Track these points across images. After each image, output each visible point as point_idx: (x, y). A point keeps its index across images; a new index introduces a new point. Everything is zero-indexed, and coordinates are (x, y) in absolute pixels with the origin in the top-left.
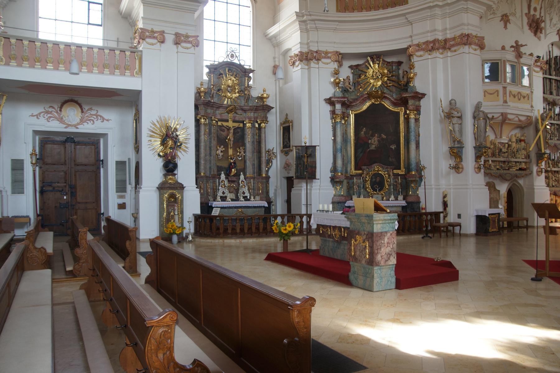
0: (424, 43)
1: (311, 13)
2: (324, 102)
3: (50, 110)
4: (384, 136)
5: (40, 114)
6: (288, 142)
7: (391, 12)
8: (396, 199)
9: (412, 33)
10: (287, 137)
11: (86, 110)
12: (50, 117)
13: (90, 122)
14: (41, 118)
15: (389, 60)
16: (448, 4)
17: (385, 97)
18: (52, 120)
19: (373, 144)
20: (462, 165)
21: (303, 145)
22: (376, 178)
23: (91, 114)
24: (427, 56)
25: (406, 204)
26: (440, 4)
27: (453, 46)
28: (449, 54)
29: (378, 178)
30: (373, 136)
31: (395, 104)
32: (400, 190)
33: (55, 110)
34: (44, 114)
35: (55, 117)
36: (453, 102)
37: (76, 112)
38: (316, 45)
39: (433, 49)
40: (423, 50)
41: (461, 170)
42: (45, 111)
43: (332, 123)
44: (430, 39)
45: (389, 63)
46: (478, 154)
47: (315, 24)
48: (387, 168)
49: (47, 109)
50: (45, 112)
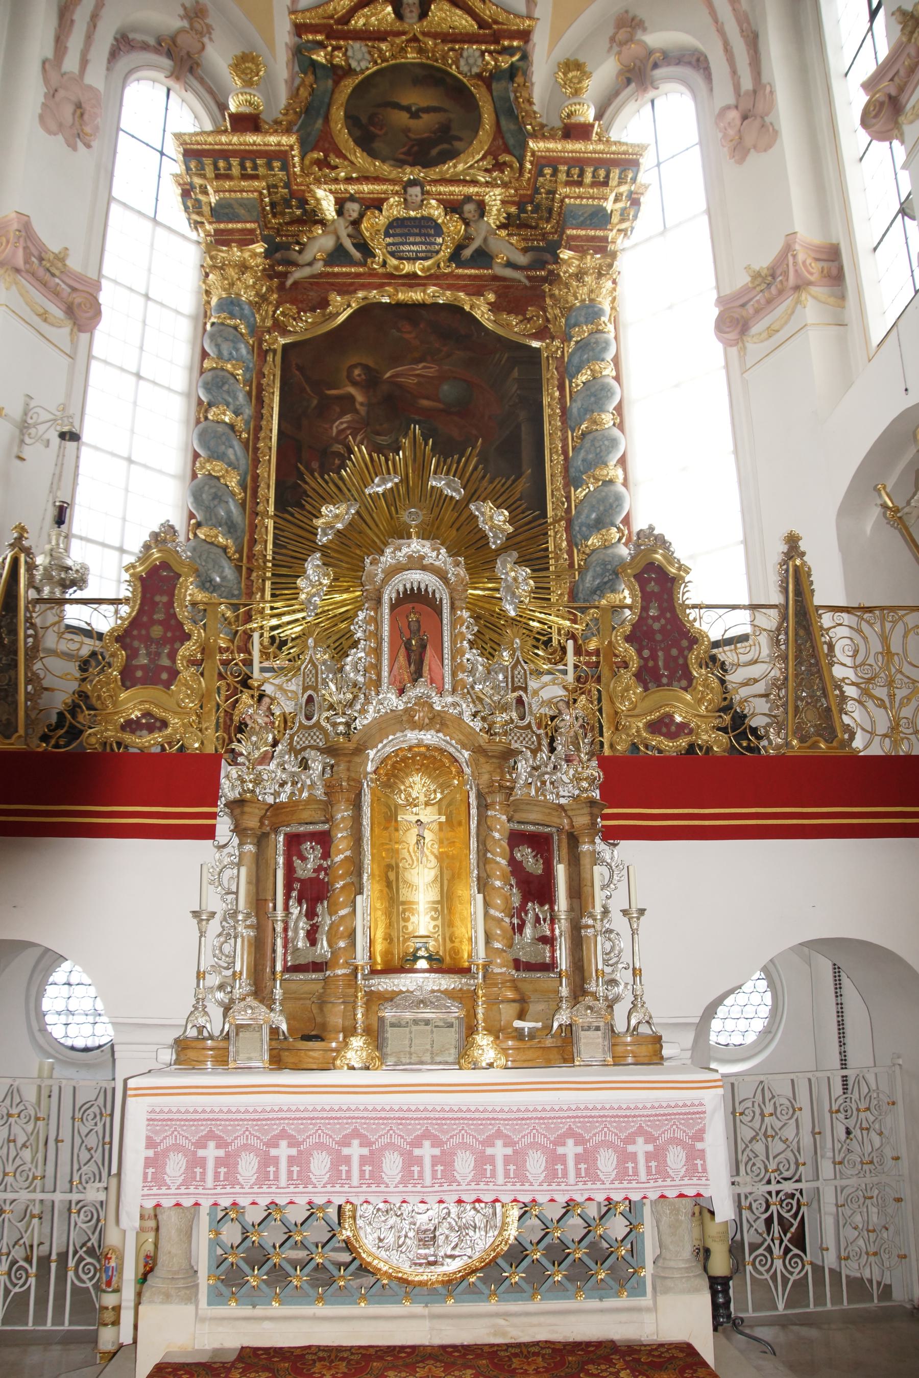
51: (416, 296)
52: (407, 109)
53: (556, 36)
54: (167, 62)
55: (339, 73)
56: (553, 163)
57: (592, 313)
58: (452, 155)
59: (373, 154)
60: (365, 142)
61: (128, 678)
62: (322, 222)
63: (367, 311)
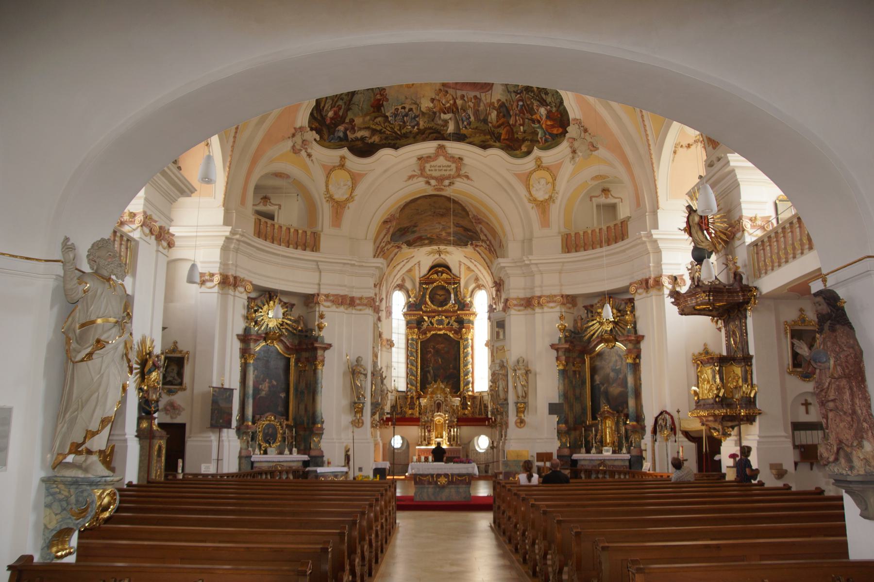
0: (334, 295)
1: (245, 234)
2: (235, 338)
4: (275, 383)
6: (176, 377)
7: (299, 253)
8: (291, 453)
9: (320, 280)
10: (175, 371)
15: (285, 300)
16: (362, 266)
17: (281, 341)
19: (263, 390)
20: (363, 420)
21: (221, 386)
22: (269, 429)
24: (334, 308)
25: (309, 459)
26: (356, 264)
27: (359, 305)
28: (354, 311)
29: (271, 429)
30: (264, 381)
31: (287, 348)
32: (294, 443)
36: (360, 359)
38: (234, 268)
39: (342, 304)
40: (333, 302)
41: (360, 425)
43: (241, 364)
44: (342, 293)
45: (285, 303)
46: (374, 411)
47: (239, 245)
48: (279, 419)
51: (442, 332)
52: (439, 295)
53: (465, 278)
54: (398, 288)
55: (427, 289)
56: (462, 314)
57: (467, 340)
58: (446, 304)
59: (434, 305)
60: (432, 302)
61: (410, 409)
62: (426, 321)
63: (433, 334)
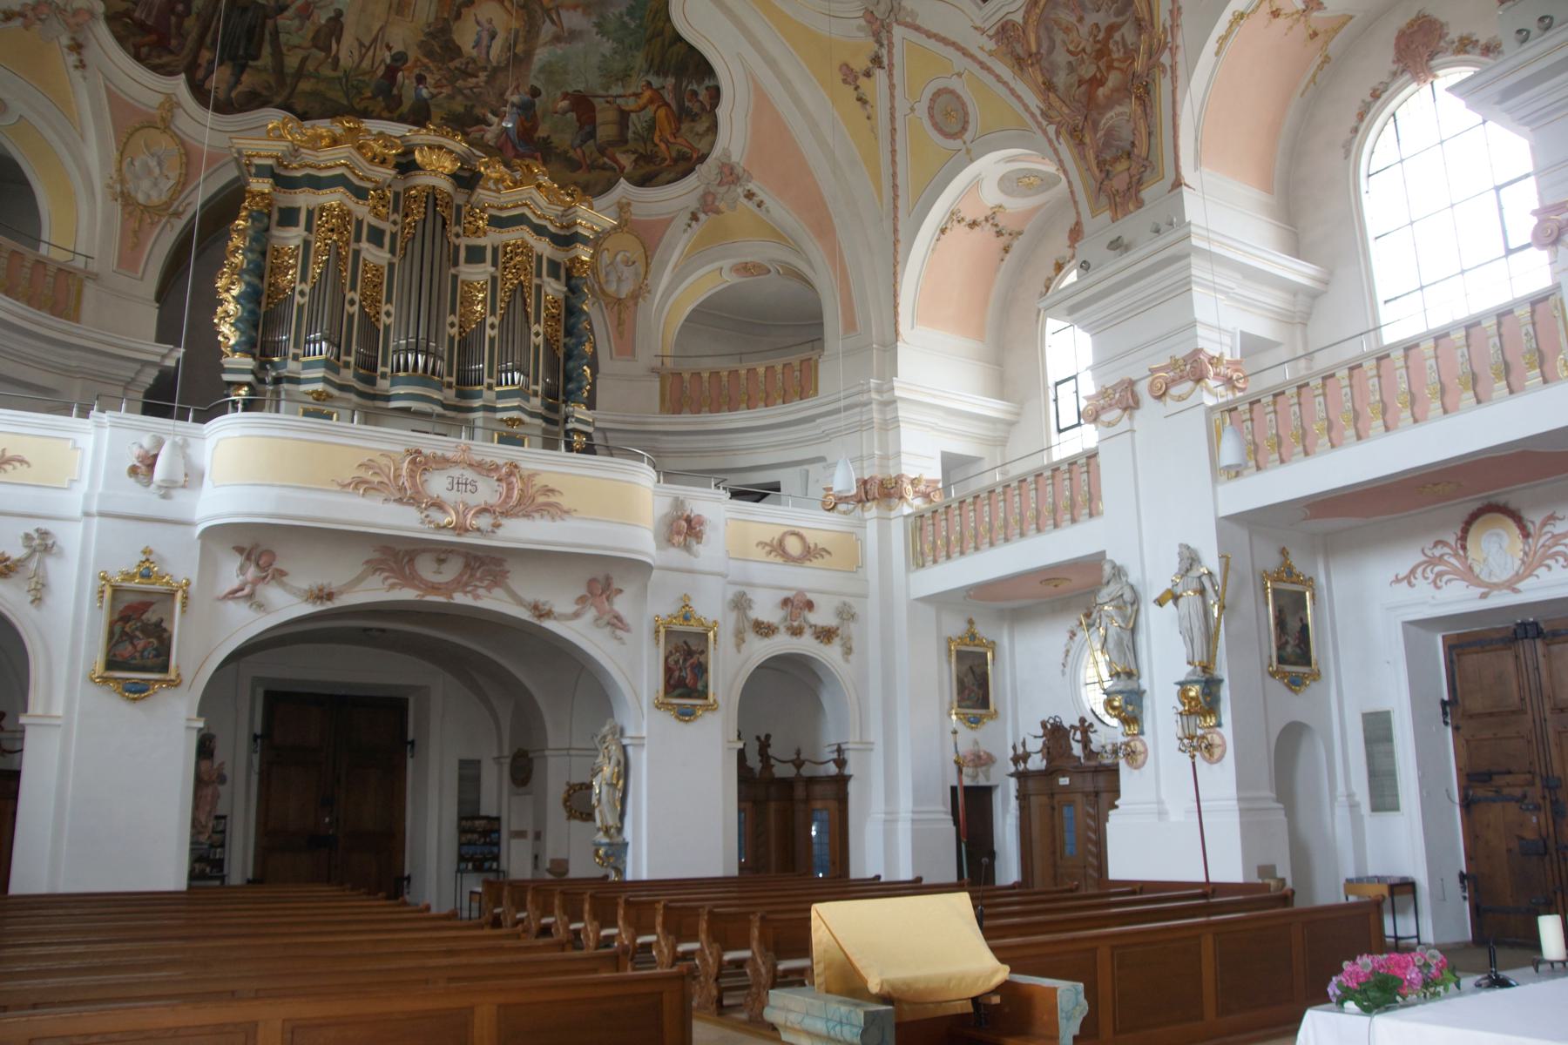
3: (1438, 552)
5: (1413, 572)
11: (1538, 524)
12: (1440, 575)
13: (1557, 561)
14: (1419, 582)
18: (1446, 583)
23: (1554, 536)
33: (1451, 548)
34: (1424, 570)
35: (1455, 571)
37: (1506, 542)
42: (1424, 558)
49: (1429, 553)
50: (1425, 562)
